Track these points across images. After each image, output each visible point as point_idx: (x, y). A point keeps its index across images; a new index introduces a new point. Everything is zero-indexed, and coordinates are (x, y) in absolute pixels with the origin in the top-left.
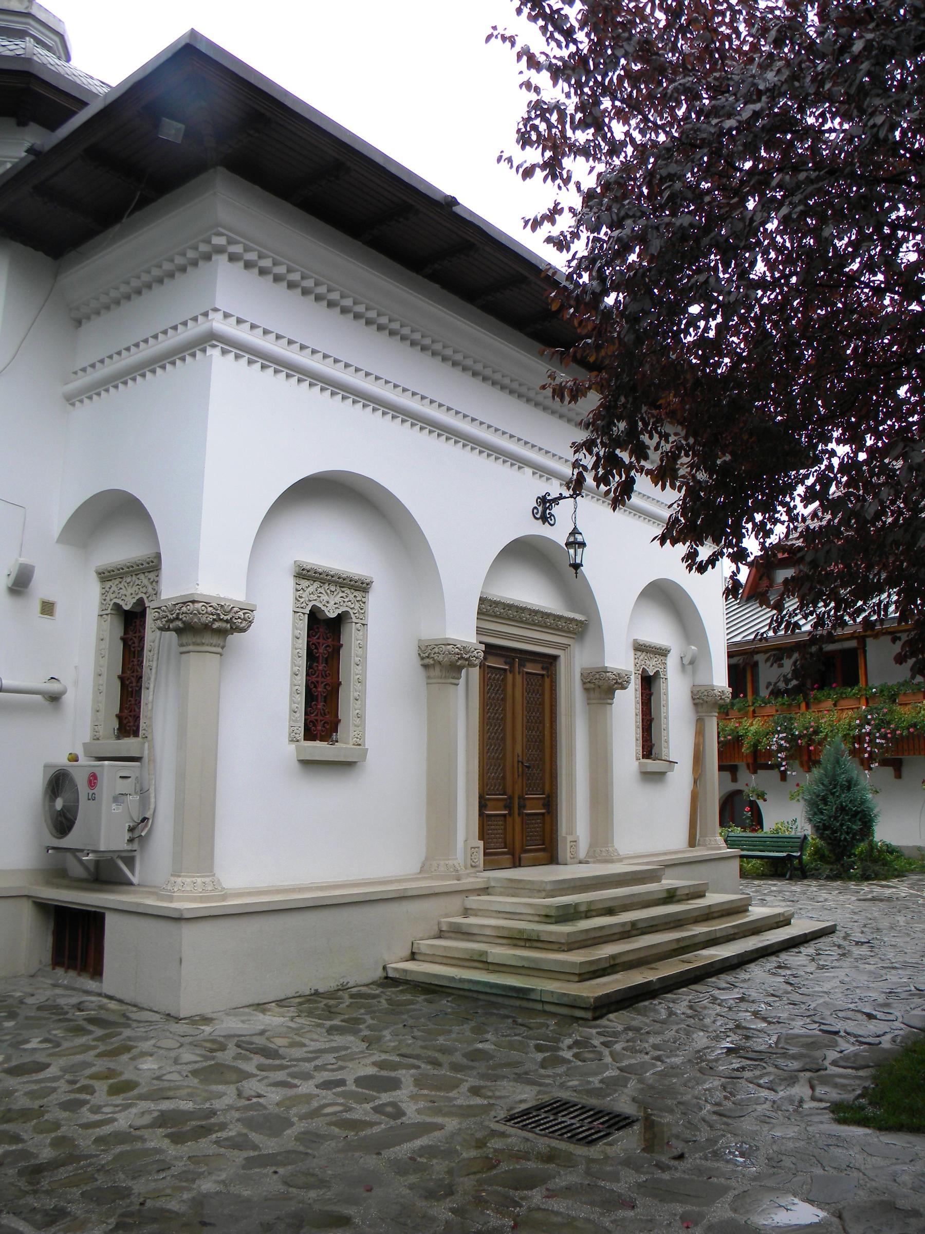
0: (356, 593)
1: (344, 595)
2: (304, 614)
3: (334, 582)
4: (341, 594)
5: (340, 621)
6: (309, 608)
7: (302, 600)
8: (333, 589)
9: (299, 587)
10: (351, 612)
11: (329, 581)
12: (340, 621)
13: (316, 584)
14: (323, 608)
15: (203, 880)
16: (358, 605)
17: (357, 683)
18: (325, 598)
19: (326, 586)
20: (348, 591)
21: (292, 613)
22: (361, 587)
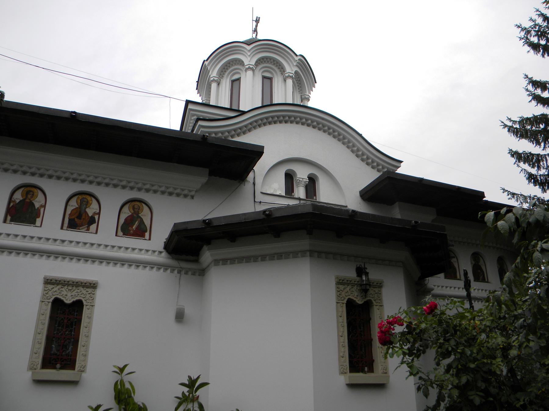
0: (88, 290)
1: (78, 291)
2: (49, 302)
3: (71, 284)
6: (52, 299)
7: (47, 295)
8: (70, 288)
9: (46, 289)
10: (83, 300)
11: (66, 284)
12: (78, 305)
13: (59, 286)
14: (62, 298)
16: (88, 296)
19: (66, 287)
20: (82, 289)
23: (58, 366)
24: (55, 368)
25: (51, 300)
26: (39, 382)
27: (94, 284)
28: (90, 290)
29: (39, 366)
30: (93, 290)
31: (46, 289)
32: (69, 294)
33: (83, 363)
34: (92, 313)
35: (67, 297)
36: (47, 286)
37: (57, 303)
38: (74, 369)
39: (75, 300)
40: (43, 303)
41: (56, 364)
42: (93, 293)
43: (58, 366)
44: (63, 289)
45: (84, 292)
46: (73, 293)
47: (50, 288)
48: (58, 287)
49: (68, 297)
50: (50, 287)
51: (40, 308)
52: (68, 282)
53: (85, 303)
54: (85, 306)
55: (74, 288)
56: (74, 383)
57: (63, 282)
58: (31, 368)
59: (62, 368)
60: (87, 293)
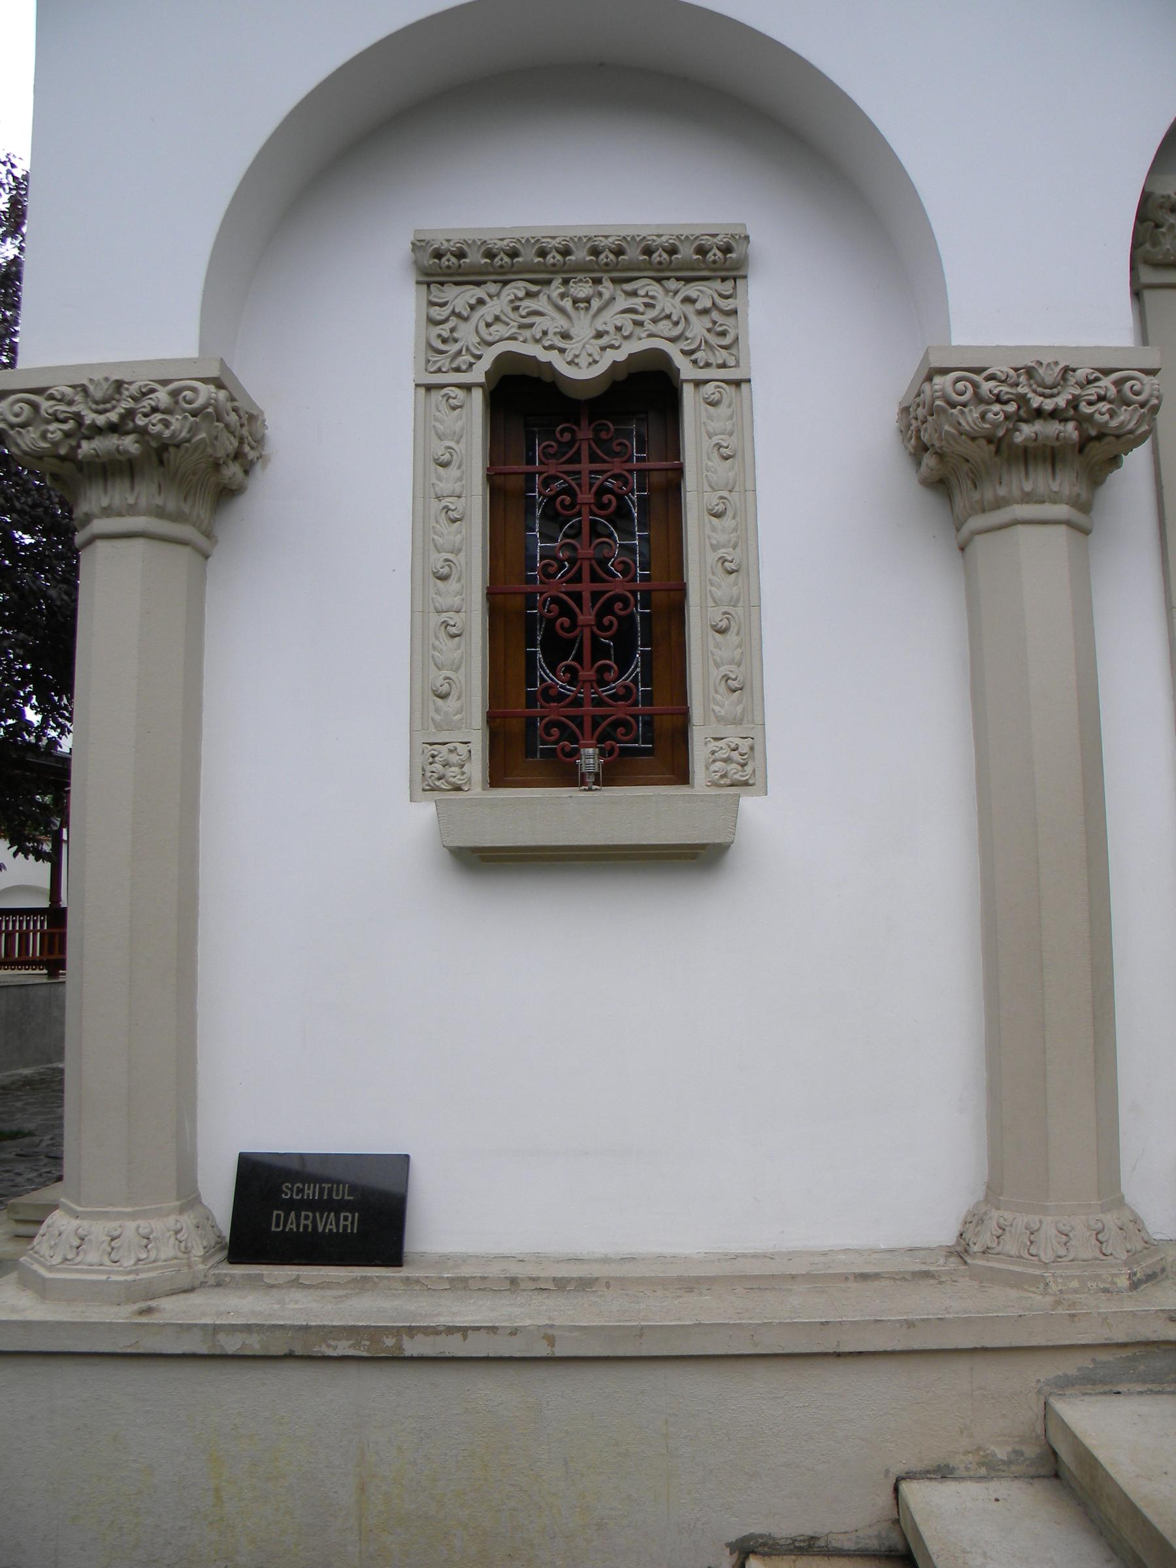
0: (692, 290)
1: (637, 303)
2: (467, 388)
4: (623, 303)
5: (647, 395)
6: (485, 364)
7: (453, 348)
8: (583, 290)
9: (438, 313)
10: (673, 351)
11: (554, 269)
12: (647, 395)
13: (517, 289)
14: (544, 356)
15: (144, 1225)
16: (698, 328)
17: (720, 577)
18: (553, 322)
19: (556, 289)
20: (655, 289)
21: (406, 398)
22: (718, 263)
23: (590, 758)
24: (569, 776)
25: (478, 374)
26: (482, 861)
27: (727, 249)
28: (705, 293)
29: (477, 769)
30: (727, 287)
31: (438, 313)
32: (582, 328)
33: (733, 736)
34: (742, 425)
35: (572, 347)
36: (437, 295)
37: (522, 400)
38: (681, 775)
39: (621, 356)
40: (436, 396)
41: (575, 753)
42: (725, 304)
43: (590, 758)
44: (540, 304)
45: (672, 305)
46: (609, 319)
47: (461, 306)
48: (510, 291)
49: (583, 347)
50: (460, 297)
51: (425, 428)
52: (566, 252)
53: (686, 369)
54: (688, 392)
55: (607, 288)
56: (697, 858)
57: (528, 256)
58: (431, 781)
59: (612, 774)
60: (689, 309)
